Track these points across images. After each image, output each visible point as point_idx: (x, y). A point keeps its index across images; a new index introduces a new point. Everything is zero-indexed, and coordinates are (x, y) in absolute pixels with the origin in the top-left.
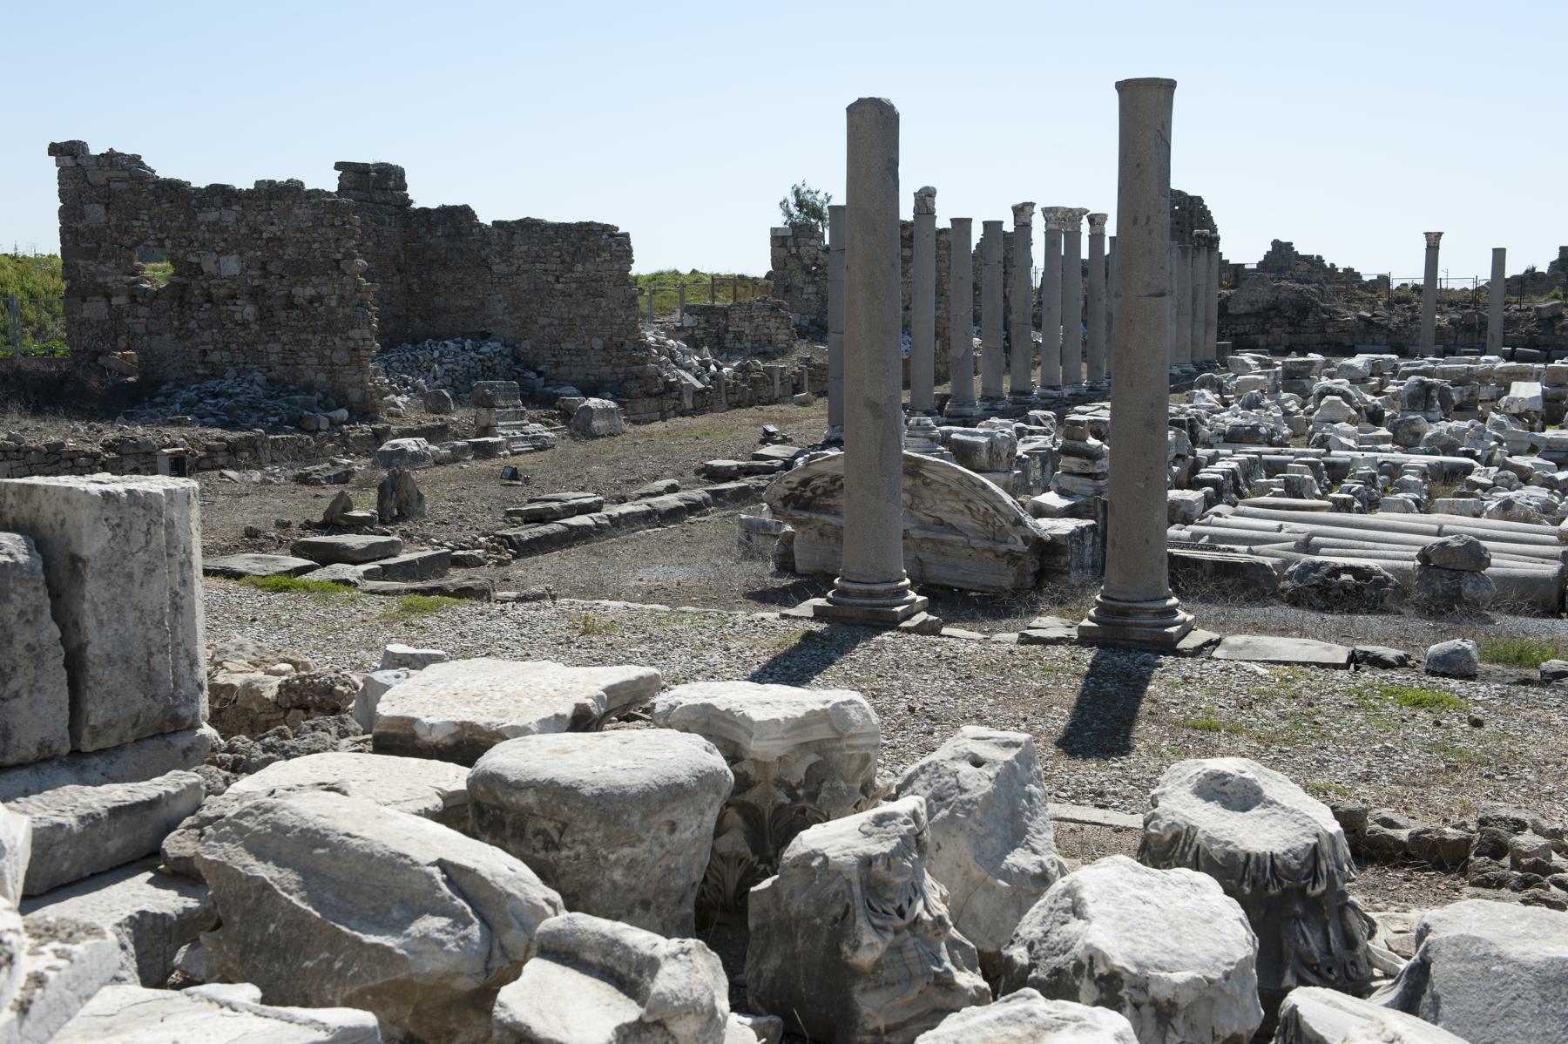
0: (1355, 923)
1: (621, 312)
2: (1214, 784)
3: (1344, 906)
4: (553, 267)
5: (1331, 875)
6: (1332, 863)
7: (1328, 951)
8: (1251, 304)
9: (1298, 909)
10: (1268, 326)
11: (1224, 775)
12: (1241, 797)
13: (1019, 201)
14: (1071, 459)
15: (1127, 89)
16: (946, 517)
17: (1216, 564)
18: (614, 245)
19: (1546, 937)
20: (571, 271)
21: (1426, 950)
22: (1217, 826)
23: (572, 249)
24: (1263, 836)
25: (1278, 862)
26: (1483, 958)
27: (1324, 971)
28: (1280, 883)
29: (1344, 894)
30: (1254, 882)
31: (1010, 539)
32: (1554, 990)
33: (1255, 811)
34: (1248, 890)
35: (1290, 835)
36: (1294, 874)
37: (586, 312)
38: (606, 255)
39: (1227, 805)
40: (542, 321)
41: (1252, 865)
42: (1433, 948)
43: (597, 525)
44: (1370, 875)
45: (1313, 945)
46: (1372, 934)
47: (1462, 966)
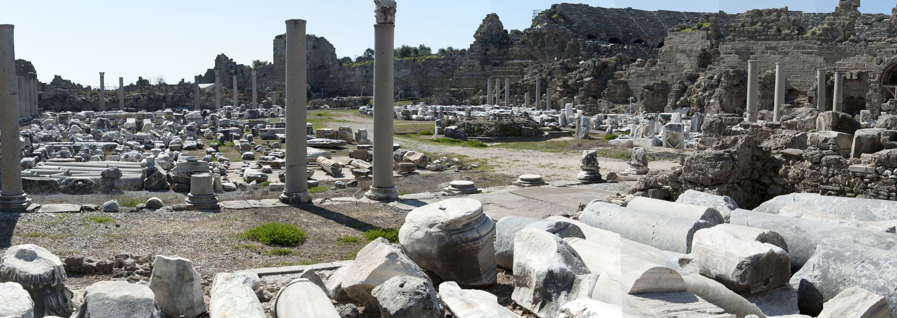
0: (67, 294)
2: (22, 253)
3: (63, 289)
5: (58, 279)
6: (59, 275)
7: (59, 304)
9: (48, 291)
11: (25, 250)
12: (29, 257)
19: (121, 290)
21: (86, 299)
22: (23, 267)
24: (38, 269)
25: (42, 277)
26: (102, 300)
27: (57, 311)
28: (42, 284)
29: (63, 285)
30: (34, 284)
32: (123, 306)
33: (35, 261)
34: (32, 287)
35: (45, 268)
36: (47, 280)
39: (26, 260)
41: (33, 279)
42: (88, 298)
44: (74, 280)
45: (53, 303)
46: (72, 298)
47: (96, 303)
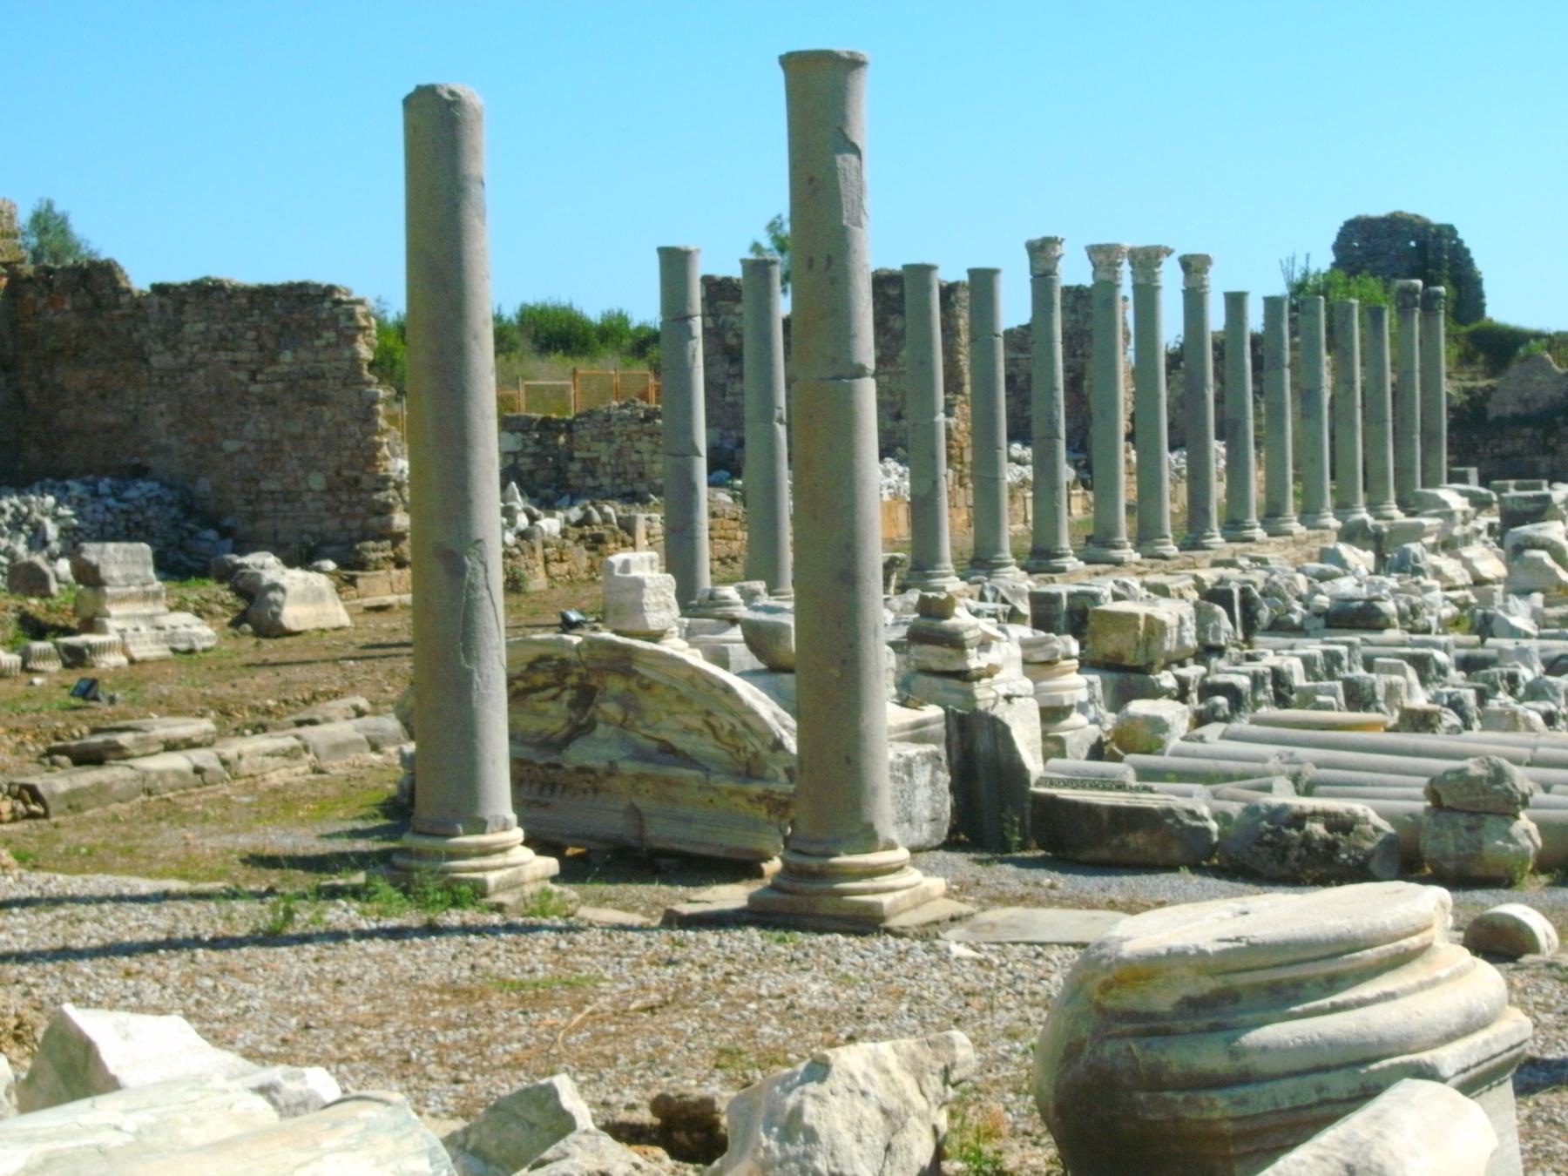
1: (354, 428)
4: (242, 356)
8: (1525, 402)
10: (1552, 441)
13: (1037, 235)
14: (927, 648)
15: (797, 65)
16: (680, 742)
17: (1115, 811)
18: (343, 318)
20: (274, 361)
23: (276, 328)
31: (769, 773)
37: (297, 429)
38: (330, 336)
40: (230, 445)
43: (198, 770)
